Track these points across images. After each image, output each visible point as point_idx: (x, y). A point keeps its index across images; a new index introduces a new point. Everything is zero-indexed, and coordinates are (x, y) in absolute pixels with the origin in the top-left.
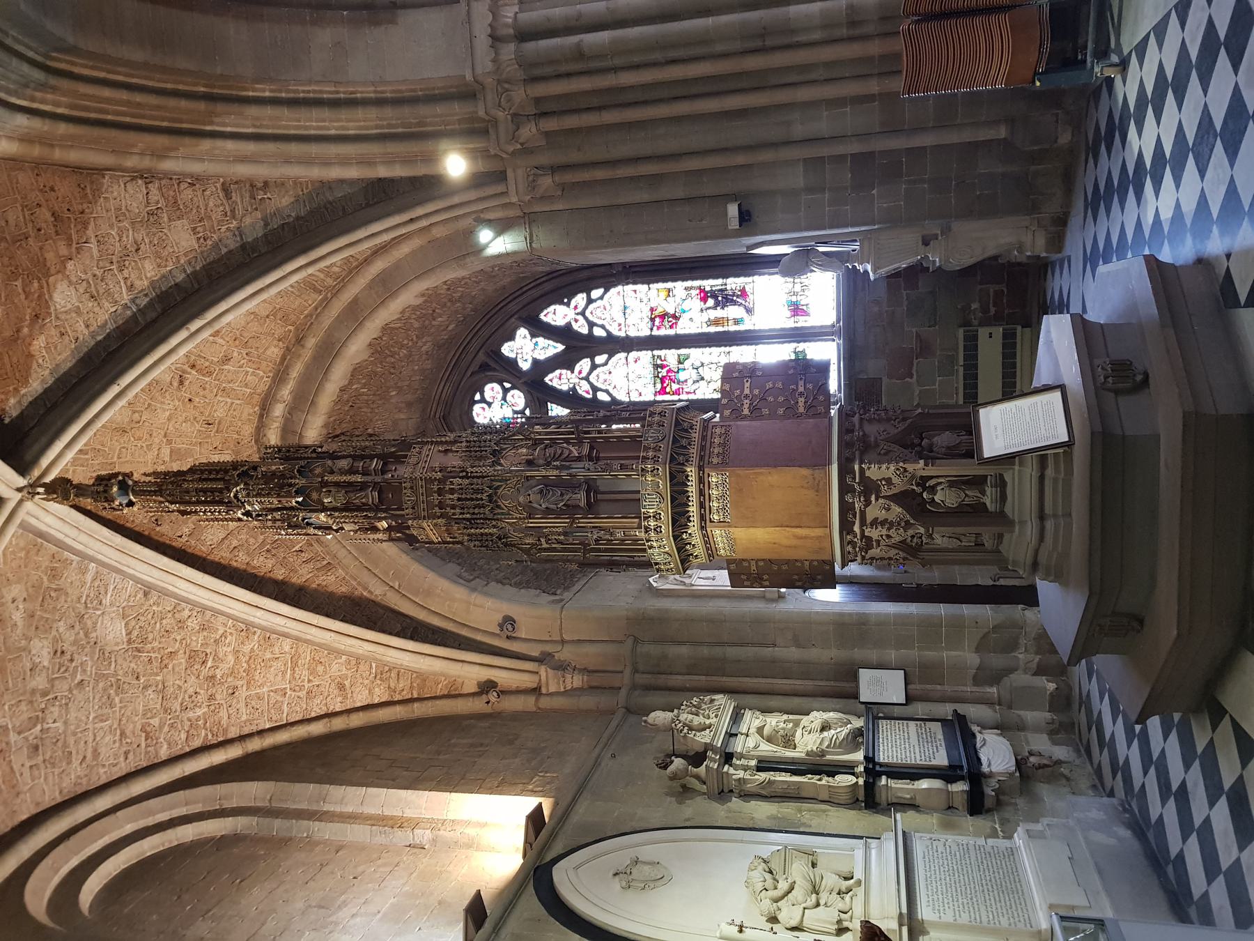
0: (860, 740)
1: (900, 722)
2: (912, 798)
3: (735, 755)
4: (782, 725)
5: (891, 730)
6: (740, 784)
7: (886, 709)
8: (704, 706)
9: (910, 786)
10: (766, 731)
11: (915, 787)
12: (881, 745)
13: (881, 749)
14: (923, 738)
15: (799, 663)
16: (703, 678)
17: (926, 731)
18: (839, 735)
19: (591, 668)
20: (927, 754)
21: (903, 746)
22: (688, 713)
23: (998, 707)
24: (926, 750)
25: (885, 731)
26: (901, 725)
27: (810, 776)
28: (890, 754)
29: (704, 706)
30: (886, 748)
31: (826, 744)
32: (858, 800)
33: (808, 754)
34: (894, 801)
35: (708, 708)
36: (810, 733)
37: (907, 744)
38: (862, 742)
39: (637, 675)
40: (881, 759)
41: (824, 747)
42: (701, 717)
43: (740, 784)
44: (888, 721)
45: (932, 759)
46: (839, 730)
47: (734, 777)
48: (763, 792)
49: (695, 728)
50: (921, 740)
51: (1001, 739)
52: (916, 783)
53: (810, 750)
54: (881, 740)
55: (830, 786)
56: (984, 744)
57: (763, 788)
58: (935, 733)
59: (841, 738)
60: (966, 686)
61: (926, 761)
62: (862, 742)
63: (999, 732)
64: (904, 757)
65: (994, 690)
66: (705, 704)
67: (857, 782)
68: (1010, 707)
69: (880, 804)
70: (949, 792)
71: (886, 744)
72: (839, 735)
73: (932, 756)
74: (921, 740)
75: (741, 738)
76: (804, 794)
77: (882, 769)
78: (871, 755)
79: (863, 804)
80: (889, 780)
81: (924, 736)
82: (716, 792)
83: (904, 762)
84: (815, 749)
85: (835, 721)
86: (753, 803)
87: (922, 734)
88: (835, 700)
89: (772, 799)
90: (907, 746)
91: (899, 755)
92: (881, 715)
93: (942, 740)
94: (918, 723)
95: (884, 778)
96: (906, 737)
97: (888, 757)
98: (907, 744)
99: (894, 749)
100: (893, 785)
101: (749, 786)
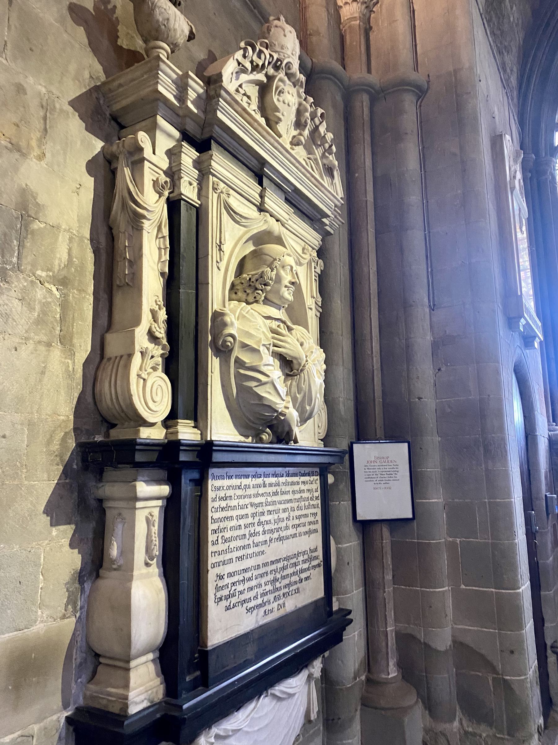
0: (265, 437)
1: (319, 518)
2: (113, 562)
3: (205, 156)
4: (287, 278)
5: (298, 500)
6: (131, 154)
7: (344, 487)
8: (318, 152)
9: (140, 555)
10: (273, 248)
11: (139, 569)
12: (260, 481)
13: (245, 481)
14: (284, 568)
15: (408, 347)
16: (370, 197)
17: (302, 571)
18: (268, 388)
19: (372, 36)
20: (240, 588)
21: (260, 529)
22: (300, 104)
23: (363, 678)
24: (253, 583)
25: (296, 488)
26: (311, 519)
27: (163, 315)
28: (234, 503)
29: (318, 152)
30: (252, 491)
31: (246, 358)
32: (113, 426)
33: (218, 316)
34: (109, 514)
35: (316, 160)
36: (273, 331)
37: (267, 537)
38: (261, 441)
39: (365, 98)
40: (218, 483)
41: (237, 353)
42: (295, 133)
43: (131, 154)
44: (318, 494)
45: (224, 603)
46: (282, 390)
47: (143, 137)
48: (116, 206)
49: (268, 99)
50: (280, 565)
51: (300, 721)
52: (155, 570)
53: (227, 319)
54: (273, 480)
55: (130, 356)
56: (279, 699)
57: (124, 205)
58: (298, 591)
59: (261, 391)
60: (396, 620)
61: (218, 588)
62: (261, 441)
63: (313, 716)
64: (227, 535)
65: (393, 672)
66: (323, 156)
67: (152, 425)
68: (365, 703)
69: (100, 480)
70: (128, 662)
71: (261, 490)
72: (268, 388)
73: (234, 600)
74: (280, 565)
75: (254, 190)
76: (118, 299)
77: (186, 487)
78: (217, 457)
79: (99, 438)
80: (160, 503)
81: (290, 571)
82: (117, 107)
83: (211, 537)
84: (230, 331)
85: (304, 387)
86: (89, 182)
87: (295, 565)
88: (351, 404)
89: (103, 230)
90: (261, 538)
91: (234, 523)
92: (331, 479)
93: (282, 612)
94: (320, 553)
95: (165, 490)
96: (283, 534)
97: (225, 498)
98: (267, 537)
99: (250, 510)
100: (140, 517)
101: (127, 171)
